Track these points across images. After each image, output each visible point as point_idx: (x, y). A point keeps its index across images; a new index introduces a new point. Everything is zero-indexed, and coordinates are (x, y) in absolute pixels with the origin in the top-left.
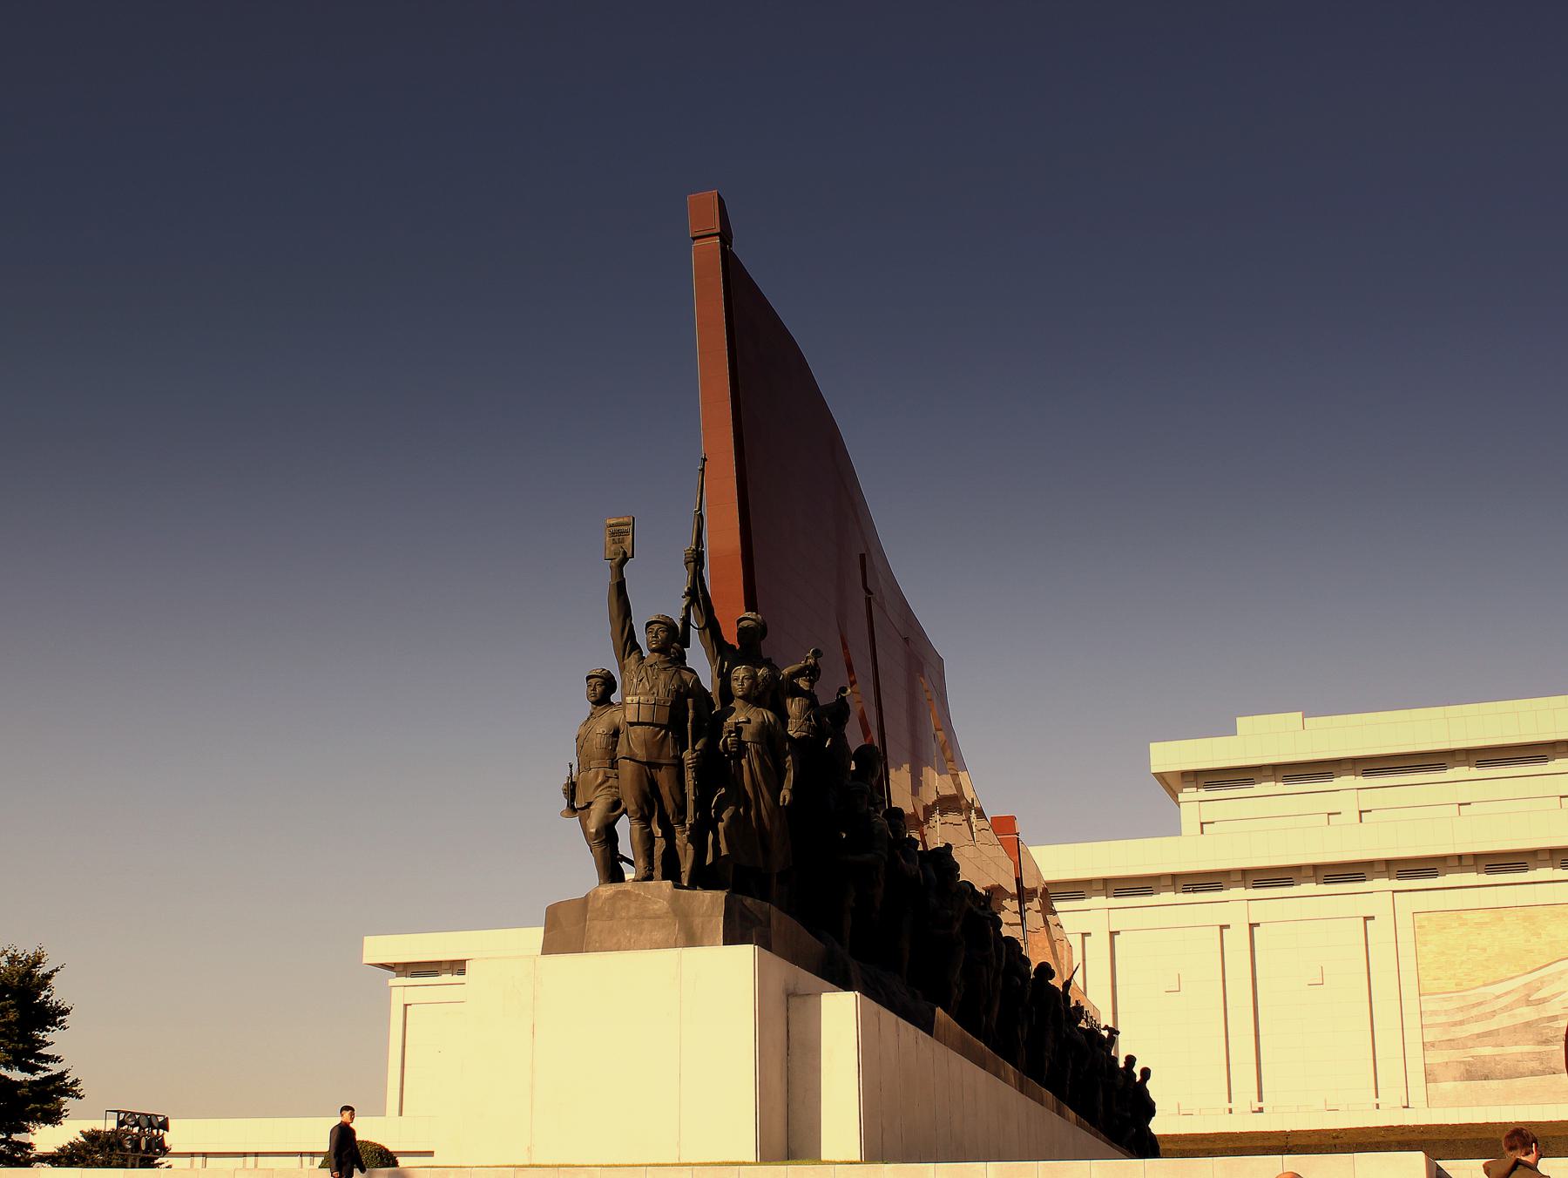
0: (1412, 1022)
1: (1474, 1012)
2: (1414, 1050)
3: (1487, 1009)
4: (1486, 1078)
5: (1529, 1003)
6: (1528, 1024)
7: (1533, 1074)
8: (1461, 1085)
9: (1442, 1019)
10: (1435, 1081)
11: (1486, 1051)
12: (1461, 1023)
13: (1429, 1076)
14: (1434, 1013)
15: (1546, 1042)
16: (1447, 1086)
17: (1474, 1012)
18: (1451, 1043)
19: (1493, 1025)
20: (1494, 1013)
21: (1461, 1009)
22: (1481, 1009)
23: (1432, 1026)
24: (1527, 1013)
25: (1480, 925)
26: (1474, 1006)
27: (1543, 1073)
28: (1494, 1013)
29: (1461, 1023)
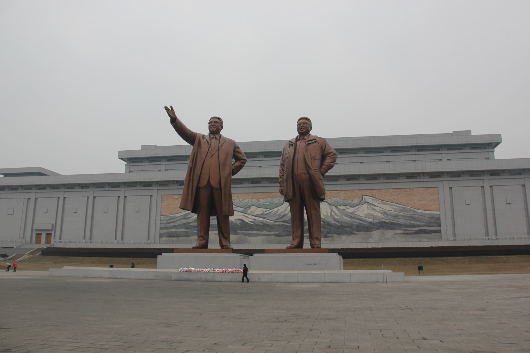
0: (158, 222)
1: (173, 220)
4: (173, 237)
5: (185, 219)
6: (184, 224)
7: (184, 236)
8: (167, 238)
12: (169, 223)
13: (161, 236)
14: (164, 220)
15: (188, 229)
16: (164, 239)
18: (166, 228)
19: (176, 224)
20: (177, 221)
21: (169, 220)
22: (174, 220)
24: (184, 221)
25: (177, 199)
27: (186, 236)
28: (177, 221)
29: (169, 223)
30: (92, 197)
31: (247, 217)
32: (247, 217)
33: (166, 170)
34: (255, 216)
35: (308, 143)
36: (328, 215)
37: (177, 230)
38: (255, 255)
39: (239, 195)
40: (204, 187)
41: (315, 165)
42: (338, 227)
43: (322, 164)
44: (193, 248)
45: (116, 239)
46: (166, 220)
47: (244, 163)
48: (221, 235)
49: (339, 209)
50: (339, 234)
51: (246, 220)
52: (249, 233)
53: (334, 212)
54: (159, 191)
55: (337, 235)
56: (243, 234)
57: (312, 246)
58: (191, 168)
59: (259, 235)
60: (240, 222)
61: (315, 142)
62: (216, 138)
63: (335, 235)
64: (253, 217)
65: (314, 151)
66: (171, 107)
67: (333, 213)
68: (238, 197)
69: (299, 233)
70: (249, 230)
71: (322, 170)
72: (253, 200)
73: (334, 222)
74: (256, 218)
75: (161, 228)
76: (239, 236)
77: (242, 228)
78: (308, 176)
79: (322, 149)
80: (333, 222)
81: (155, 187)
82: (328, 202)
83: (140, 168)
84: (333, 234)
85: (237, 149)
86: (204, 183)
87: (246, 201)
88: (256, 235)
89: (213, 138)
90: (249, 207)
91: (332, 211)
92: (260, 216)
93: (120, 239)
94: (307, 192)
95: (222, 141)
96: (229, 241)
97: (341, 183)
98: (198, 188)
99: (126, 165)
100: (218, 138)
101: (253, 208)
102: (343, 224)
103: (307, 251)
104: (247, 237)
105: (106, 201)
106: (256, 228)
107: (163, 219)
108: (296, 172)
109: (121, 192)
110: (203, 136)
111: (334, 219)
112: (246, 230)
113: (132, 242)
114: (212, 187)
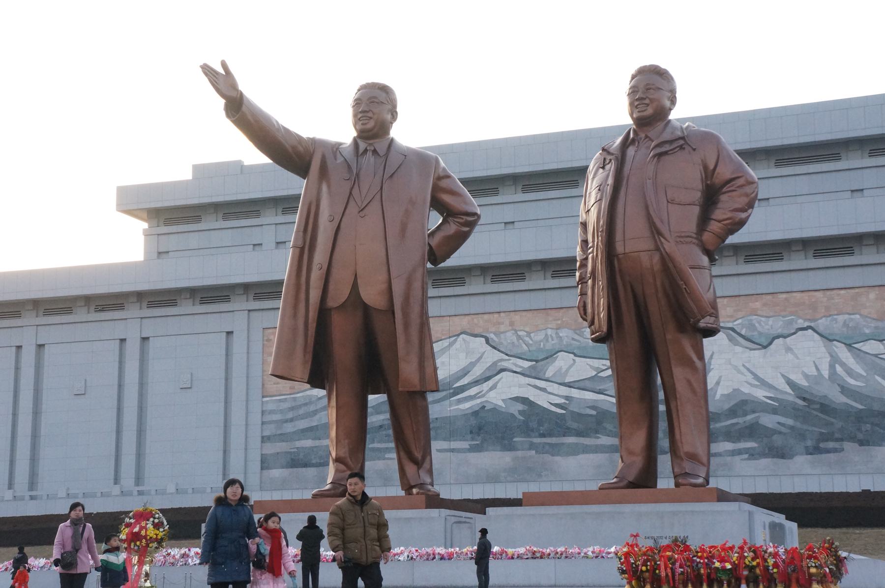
0: (256, 418)
1: (301, 412)
2: (255, 442)
3: (312, 408)
4: (305, 465)
9: (277, 417)
10: (268, 468)
11: (308, 443)
12: (292, 420)
13: (265, 463)
14: (272, 412)
16: (276, 473)
17: (301, 412)
18: (283, 437)
20: (315, 412)
21: (292, 409)
23: (270, 422)
26: (300, 406)
28: (315, 412)
29: (292, 420)
30: (33, 349)
31: (544, 390)
32: (544, 390)
33: (278, 243)
34: (569, 385)
35: (659, 150)
36: (820, 375)
37: (317, 443)
38: (489, 510)
39: (516, 317)
40: (343, 306)
41: (682, 219)
42: (859, 417)
43: (704, 219)
44: (315, 496)
45: (116, 481)
46: (281, 412)
47: (472, 225)
48: (402, 453)
49: (859, 355)
50: (862, 443)
51: (543, 400)
52: (551, 445)
53: (843, 365)
54: (252, 314)
55: (856, 445)
56: (532, 446)
57: (680, 477)
58: (302, 249)
59: (586, 450)
60: (520, 407)
61: (681, 147)
62: (375, 152)
63: (848, 446)
64: (564, 391)
65: (685, 175)
66: (224, 65)
67: (839, 369)
68: (512, 324)
69: (639, 440)
70: (551, 435)
71: (706, 236)
72: (563, 333)
73: (843, 399)
74: (575, 393)
75: (264, 439)
76: (519, 453)
77: (527, 430)
78: (656, 258)
79: (705, 167)
80: (839, 399)
81: (240, 304)
82: (821, 329)
83: (194, 240)
84: (842, 440)
85: (444, 183)
86: (339, 294)
87: (540, 336)
88: (575, 450)
89: (366, 151)
90: (551, 356)
91: (835, 360)
92: (588, 384)
93: (132, 482)
94: (657, 309)
95: (394, 161)
96: (430, 472)
97: (864, 259)
98: (324, 313)
99: (147, 234)
100: (382, 151)
101: (563, 361)
102: (876, 407)
103: (668, 497)
104: (548, 457)
105: (82, 355)
106: (575, 425)
107: (270, 407)
108: (619, 248)
109: (130, 324)
110: (336, 148)
111: (844, 389)
112: (543, 435)
113: (171, 489)
114: (366, 308)
